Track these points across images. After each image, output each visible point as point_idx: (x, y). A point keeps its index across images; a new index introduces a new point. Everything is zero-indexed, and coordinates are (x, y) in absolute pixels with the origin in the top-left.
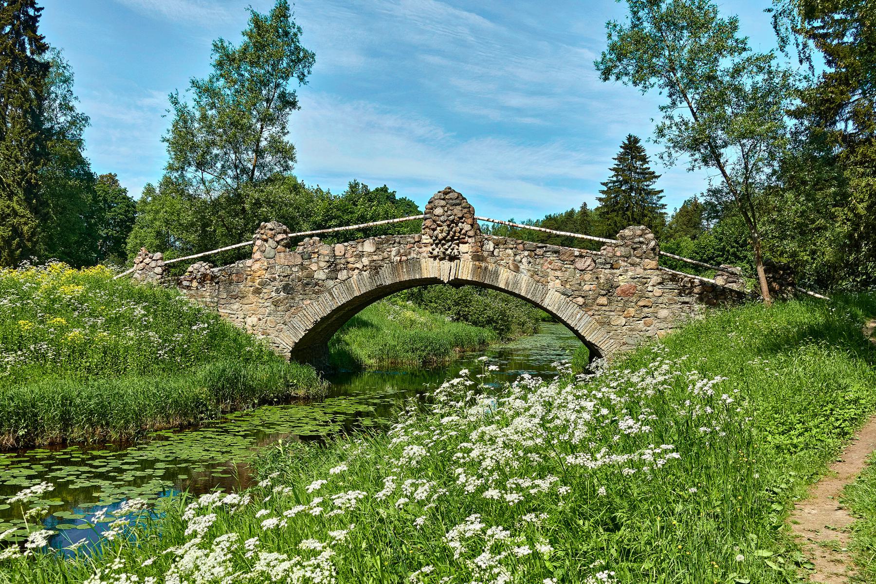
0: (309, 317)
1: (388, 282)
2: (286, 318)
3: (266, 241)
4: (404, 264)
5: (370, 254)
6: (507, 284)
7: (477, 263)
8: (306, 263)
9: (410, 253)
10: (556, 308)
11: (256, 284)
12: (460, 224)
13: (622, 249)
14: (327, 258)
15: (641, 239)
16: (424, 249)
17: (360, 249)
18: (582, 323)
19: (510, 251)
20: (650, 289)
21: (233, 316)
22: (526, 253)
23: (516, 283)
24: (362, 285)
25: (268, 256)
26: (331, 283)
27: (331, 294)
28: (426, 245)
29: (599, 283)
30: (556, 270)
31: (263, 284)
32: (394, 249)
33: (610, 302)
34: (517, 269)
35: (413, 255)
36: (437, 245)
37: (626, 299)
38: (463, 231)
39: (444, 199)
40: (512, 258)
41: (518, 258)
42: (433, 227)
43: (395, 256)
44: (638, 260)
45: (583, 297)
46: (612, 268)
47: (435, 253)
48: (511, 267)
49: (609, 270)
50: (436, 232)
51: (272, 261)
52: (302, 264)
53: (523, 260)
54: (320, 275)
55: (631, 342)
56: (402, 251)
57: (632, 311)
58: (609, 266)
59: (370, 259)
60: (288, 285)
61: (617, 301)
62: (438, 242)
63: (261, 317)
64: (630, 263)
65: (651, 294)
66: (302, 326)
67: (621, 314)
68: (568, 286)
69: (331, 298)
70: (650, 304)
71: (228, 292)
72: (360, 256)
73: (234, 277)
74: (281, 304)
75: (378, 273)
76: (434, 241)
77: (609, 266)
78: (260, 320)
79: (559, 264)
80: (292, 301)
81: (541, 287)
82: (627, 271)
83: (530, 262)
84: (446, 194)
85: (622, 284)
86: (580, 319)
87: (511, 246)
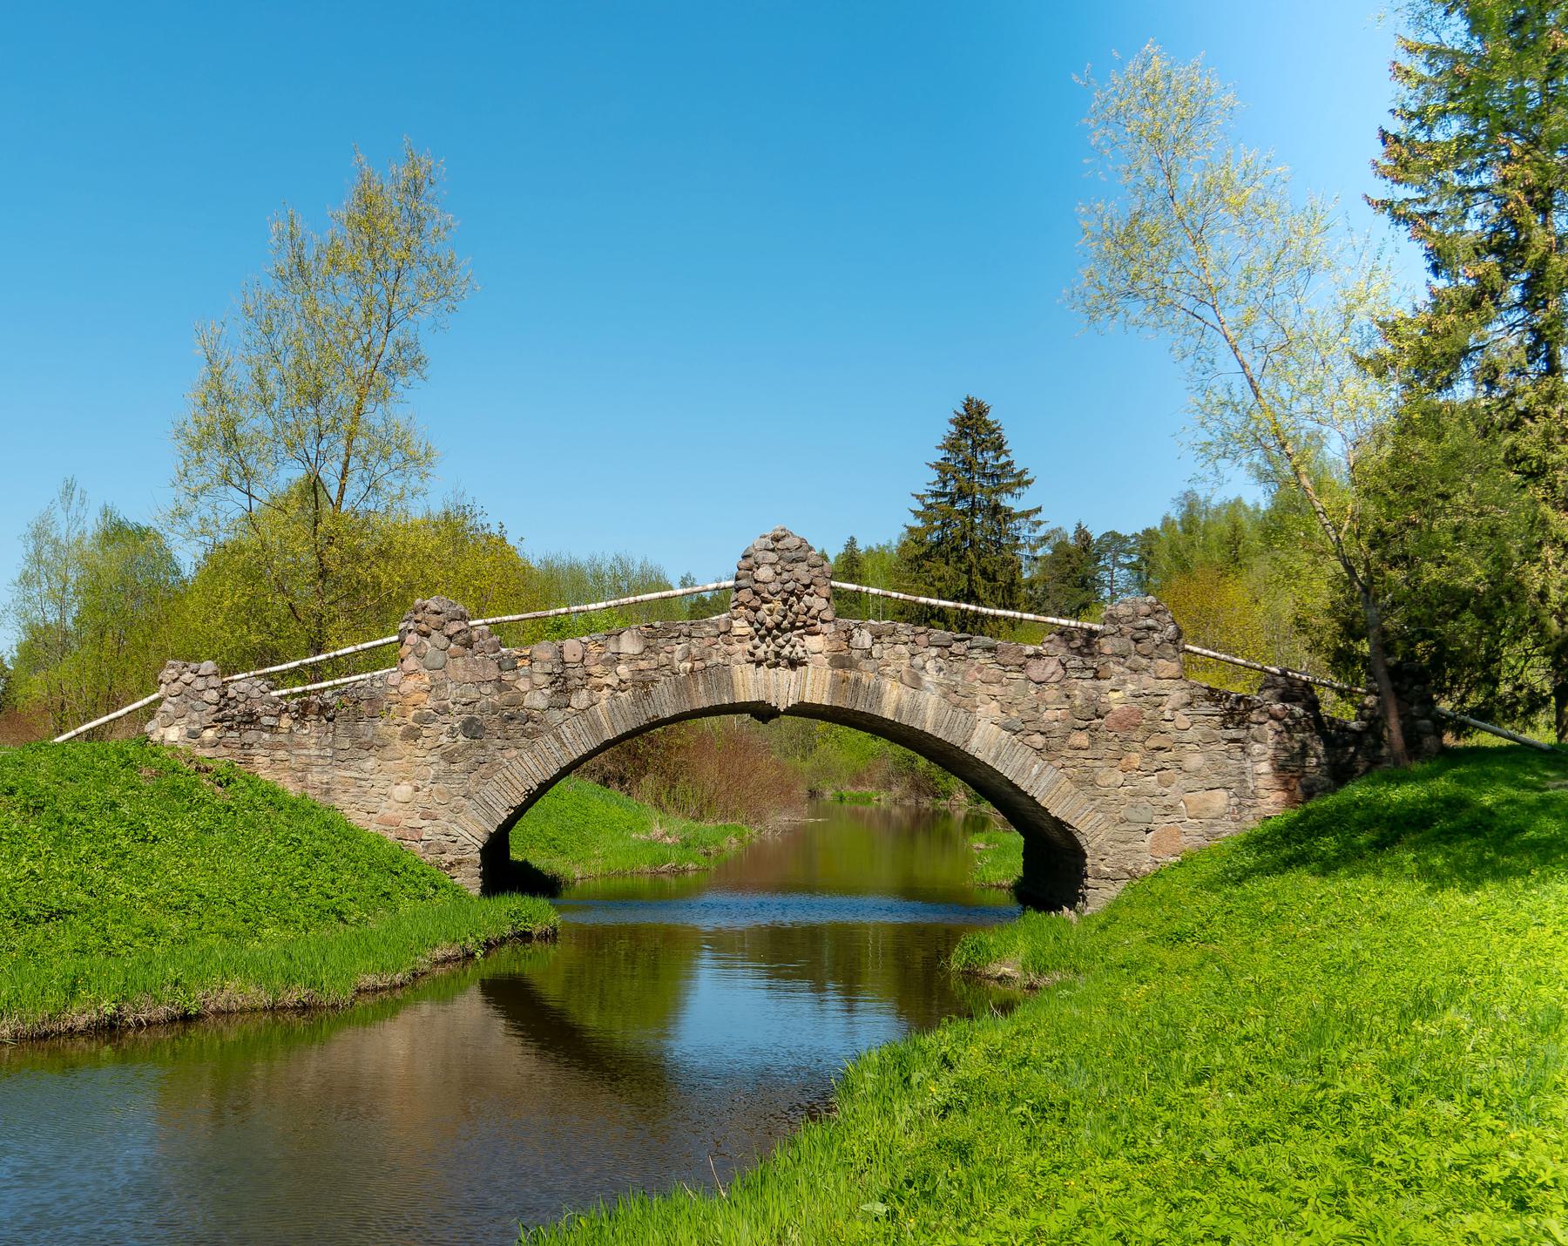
0: (514, 781)
2: (470, 784)
3: (426, 635)
4: (700, 677)
5: (632, 659)
6: (898, 710)
7: (840, 672)
8: (508, 676)
9: (710, 655)
10: (992, 755)
11: (409, 720)
12: (806, 598)
13: (1115, 640)
14: (548, 668)
15: (1150, 622)
16: (738, 646)
17: (613, 648)
19: (903, 649)
20: (1168, 715)
21: (363, 783)
22: (934, 651)
23: (915, 709)
25: (431, 665)
26: (558, 715)
27: (558, 737)
28: (741, 638)
29: (1072, 707)
30: (990, 683)
31: (424, 720)
32: (679, 647)
33: (1094, 741)
34: (916, 683)
35: (717, 659)
36: (762, 639)
37: (1122, 735)
38: (813, 612)
39: (773, 550)
40: (907, 662)
41: (918, 660)
42: (754, 603)
44: (1145, 661)
45: (1042, 733)
46: (1096, 677)
47: (760, 653)
48: (906, 678)
49: (1090, 682)
50: (760, 614)
51: (439, 675)
52: (500, 680)
53: (928, 665)
55: (1134, 817)
56: (694, 651)
57: (1136, 759)
58: (1090, 674)
59: (632, 667)
60: (472, 720)
61: (1107, 740)
62: (766, 633)
63: (420, 784)
64: (1129, 668)
65: (1169, 725)
66: (502, 800)
67: (1115, 763)
68: (1014, 714)
69: (557, 745)
70: (1167, 744)
71: (355, 737)
72: (616, 659)
73: (363, 706)
74: (459, 759)
75: (648, 694)
76: (757, 630)
77: (1090, 674)
78: (417, 789)
79: (995, 670)
80: (481, 752)
81: (962, 716)
82: (1125, 682)
83: (941, 669)
84: (778, 541)
85: (1116, 707)
86: (1038, 776)
87: (904, 638)
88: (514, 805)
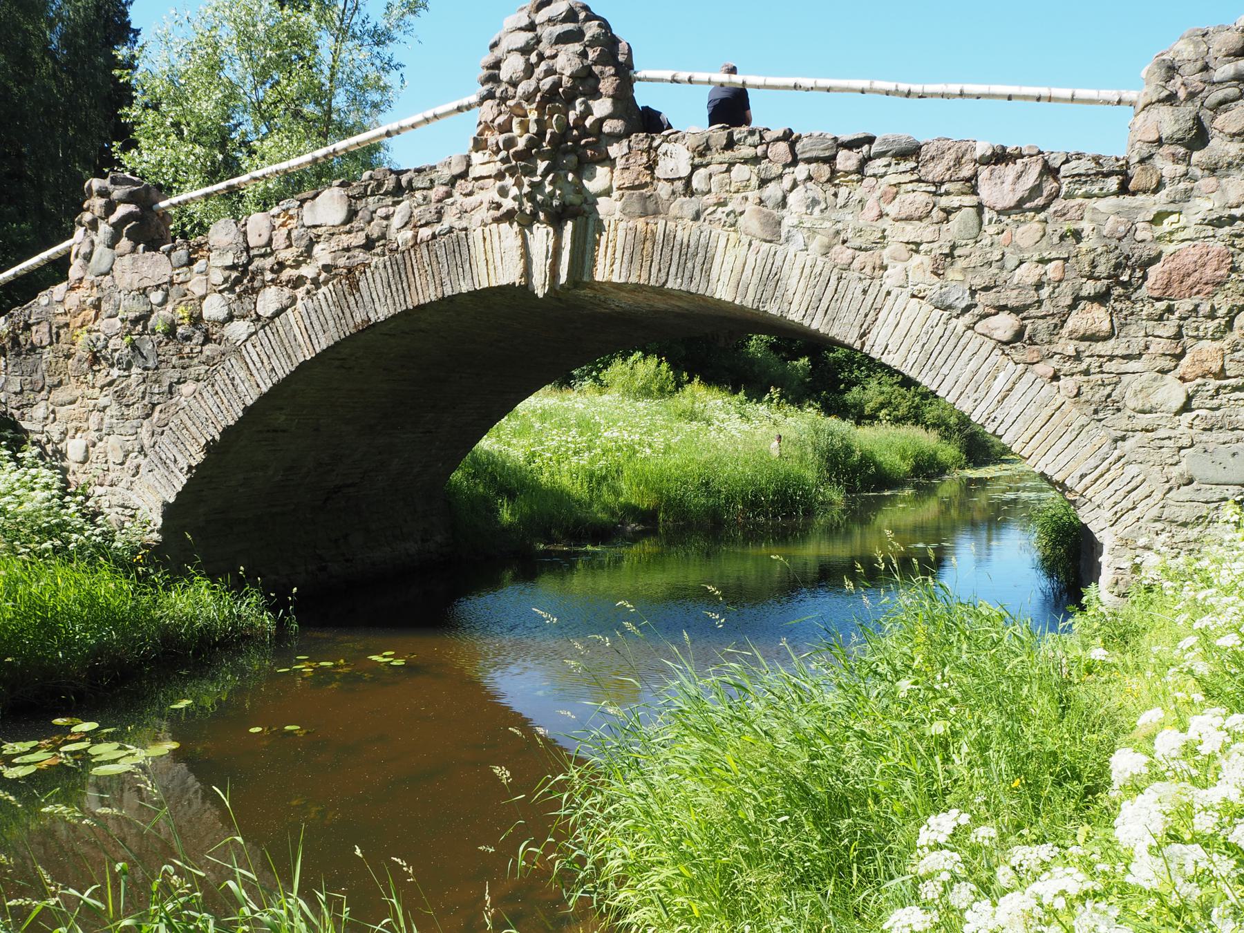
0: (193, 429)
1: (382, 312)
2: (144, 433)
7: (640, 223)
9: (440, 215)
18: (1013, 405)
19: (741, 172)
23: (772, 279)
24: (317, 327)
41: (773, 191)
43: (399, 230)
45: (1015, 310)
46: (1123, 189)
47: (508, 204)
49: (1113, 199)
54: (214, 308)
88: (194, 464)
